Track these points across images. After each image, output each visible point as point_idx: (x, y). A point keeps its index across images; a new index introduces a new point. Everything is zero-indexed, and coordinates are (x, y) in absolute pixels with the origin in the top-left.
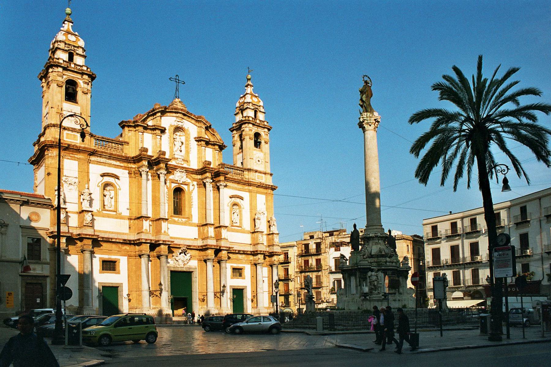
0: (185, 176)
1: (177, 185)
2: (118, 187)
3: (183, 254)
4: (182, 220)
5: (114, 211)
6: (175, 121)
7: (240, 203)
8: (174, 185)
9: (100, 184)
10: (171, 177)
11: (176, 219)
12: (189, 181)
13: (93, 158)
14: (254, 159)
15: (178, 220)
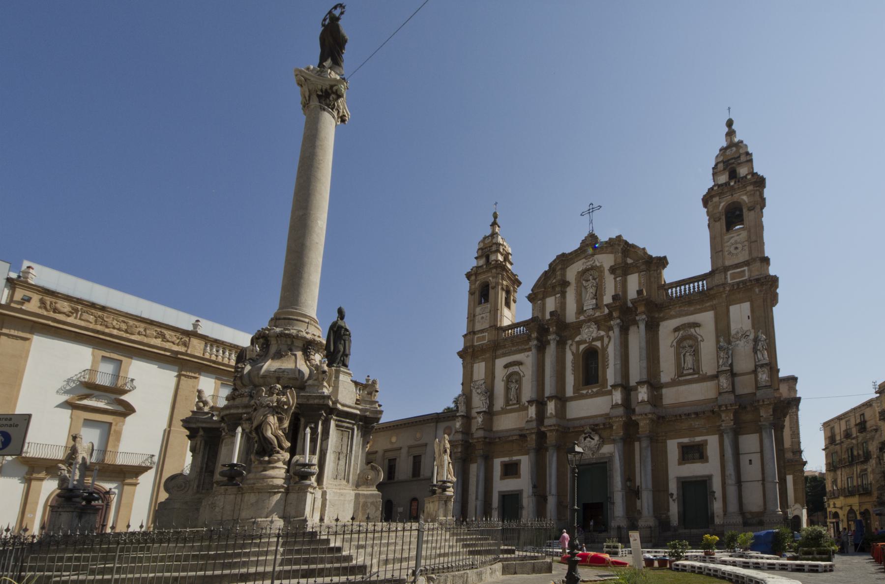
0: (595, 330)
1: (587, 345)
2: (522, 374)
3: (588, 439)
4: (592, 391)
5: (517, 404)
6: (583, 264)
7: (694, 333)
8: (582, 347)
9: (505, 379)
10: (577, 339)
11: (584, 392)
12: (602, 333)
13: (499, 352)
14: (726, 249)
15: (588, 392)
